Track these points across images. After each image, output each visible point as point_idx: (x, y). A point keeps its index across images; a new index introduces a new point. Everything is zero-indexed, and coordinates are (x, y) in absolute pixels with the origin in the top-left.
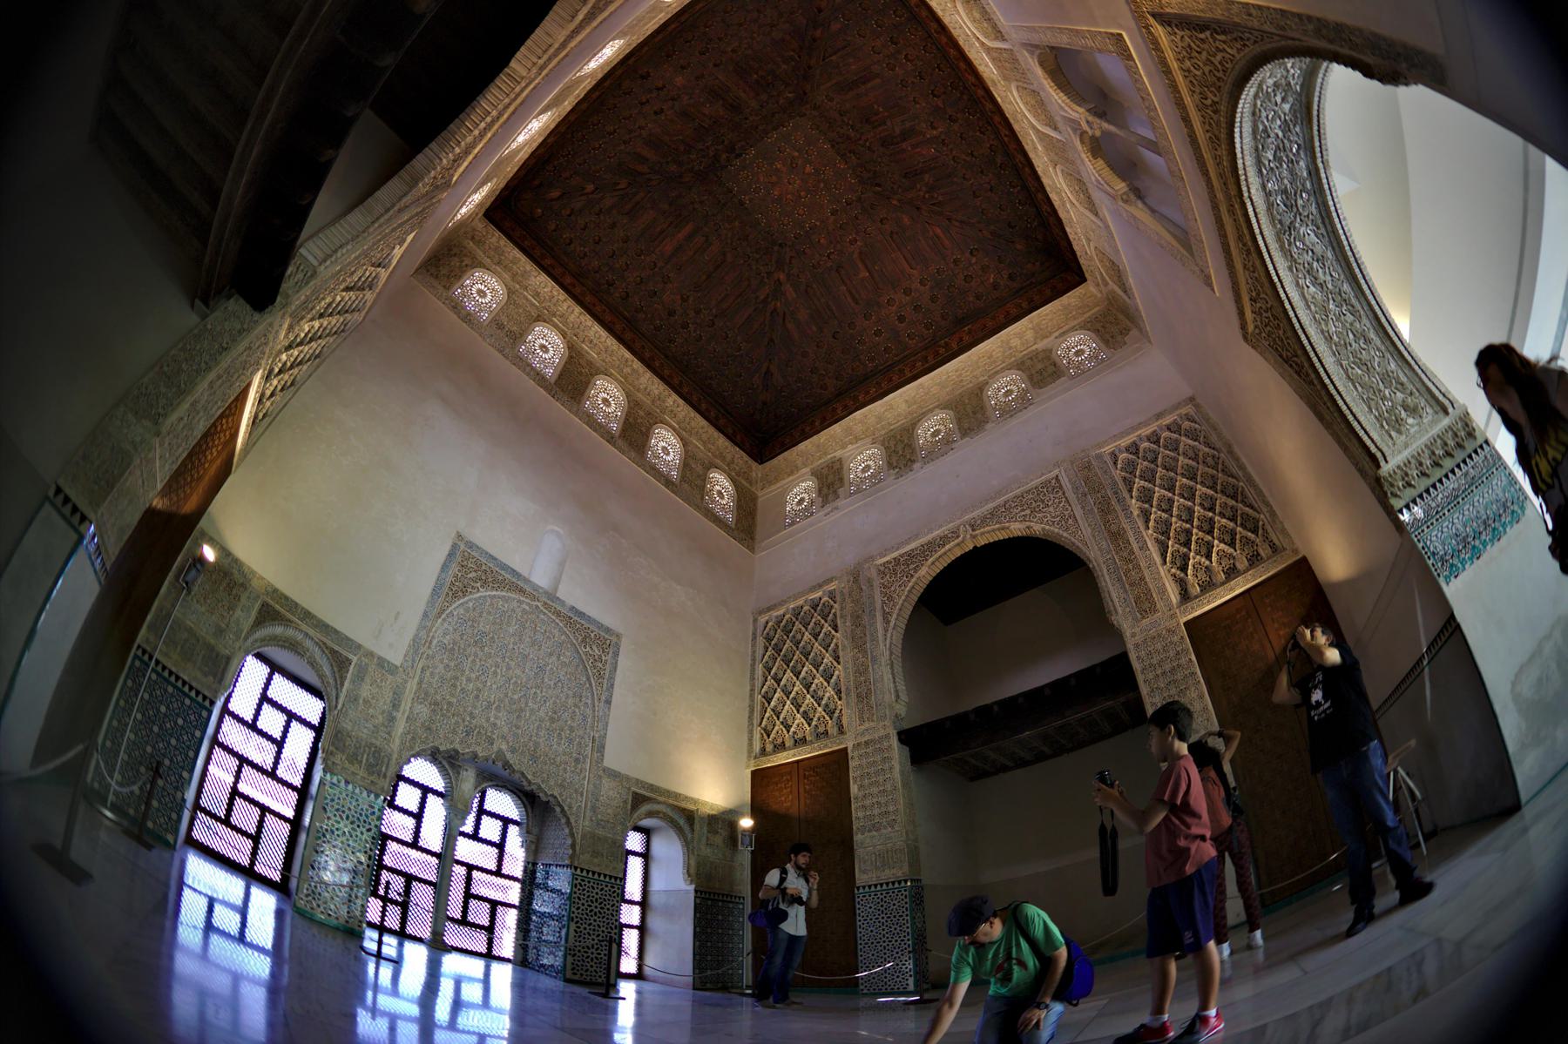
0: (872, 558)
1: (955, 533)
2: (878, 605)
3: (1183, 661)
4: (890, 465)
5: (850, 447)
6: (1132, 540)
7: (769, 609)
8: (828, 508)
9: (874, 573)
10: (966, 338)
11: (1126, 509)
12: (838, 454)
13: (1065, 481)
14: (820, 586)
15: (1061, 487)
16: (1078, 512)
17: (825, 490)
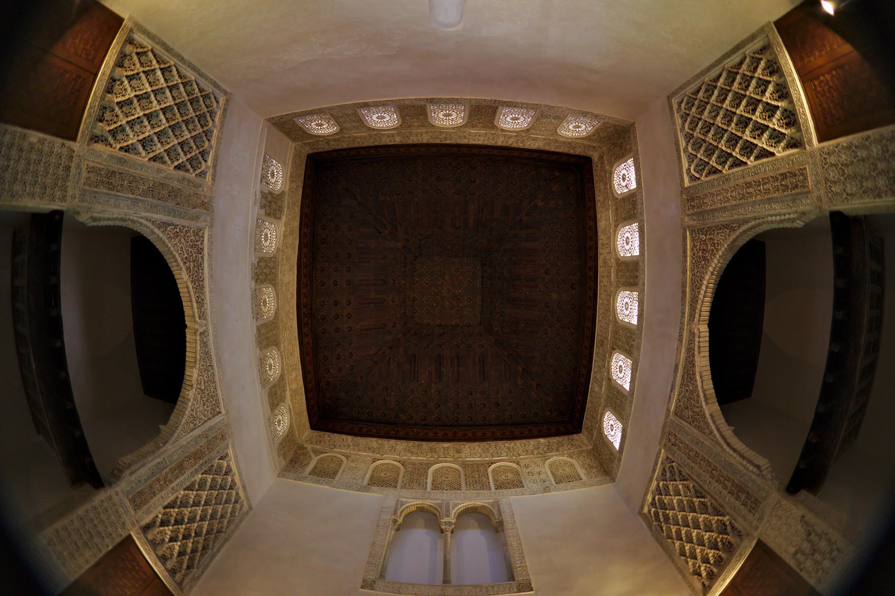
2: (176, 221)
4: (261, 260)
5: (283, 229)
8: (259, 195)
9: (200, 224)
12: (284, 219)
14: (215, 166)
17: (270, 198)
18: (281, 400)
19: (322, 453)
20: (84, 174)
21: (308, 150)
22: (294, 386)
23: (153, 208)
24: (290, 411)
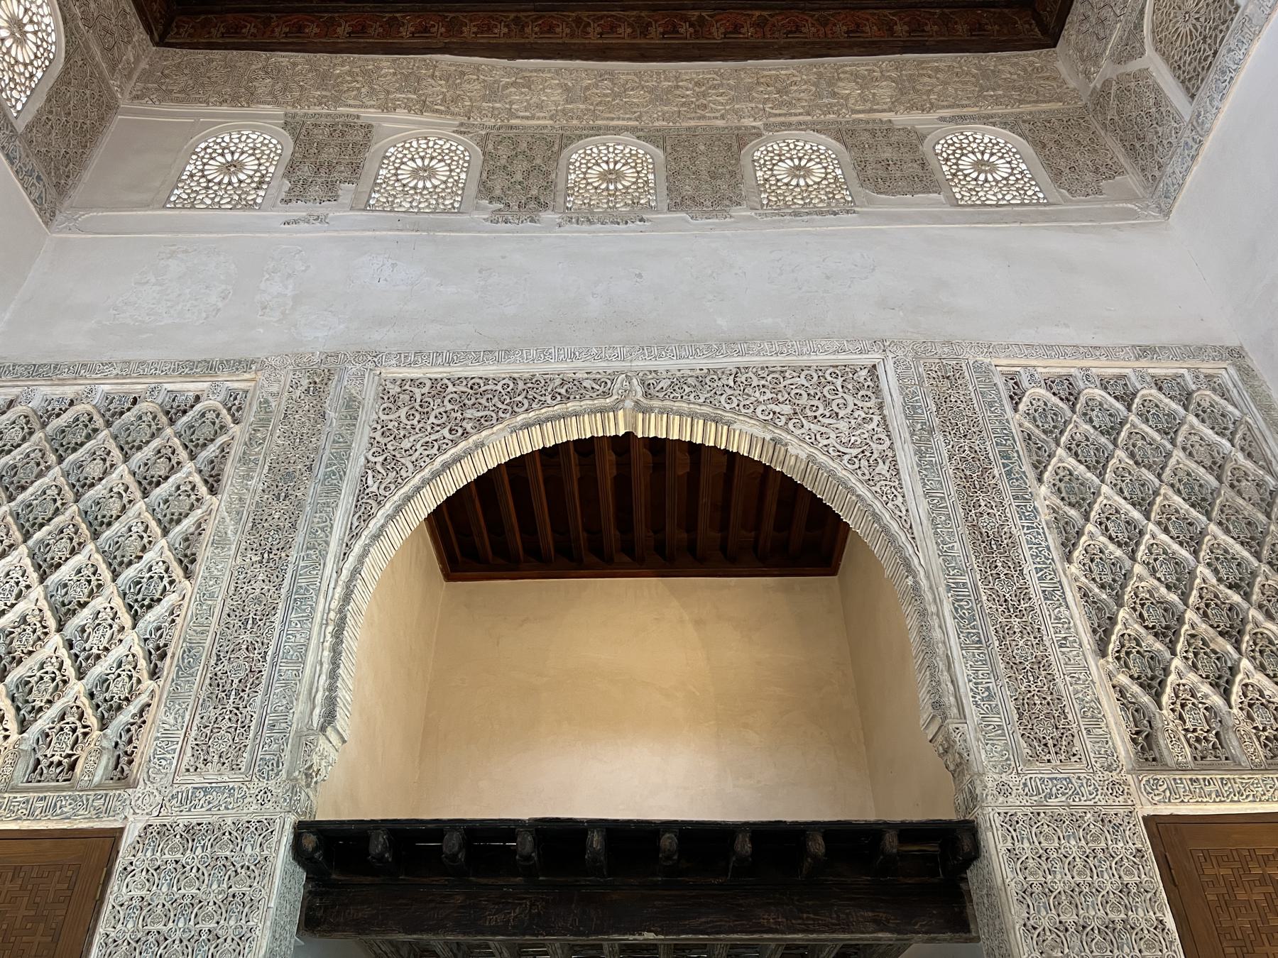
0: (376, 357)
1: (603, 385)
2: (355, 468)
3: (1139, 916)
4: (485, 189)
6: (1029, 568)
7: (36, 371)
8: (298, 210)
9: (369, 392)
10: (748, 31)
11: (1023, 497)
13: (889, 382)
14: (210, 368)
15: (877, 391)
16: (906, 458)
17: (306, 171)
18: (913, 148)
19: (1138, 26)
20: (212, 774)
21: (138, 47)
22: (885, 91)
23: (317, 547)
24: (963, 118)
